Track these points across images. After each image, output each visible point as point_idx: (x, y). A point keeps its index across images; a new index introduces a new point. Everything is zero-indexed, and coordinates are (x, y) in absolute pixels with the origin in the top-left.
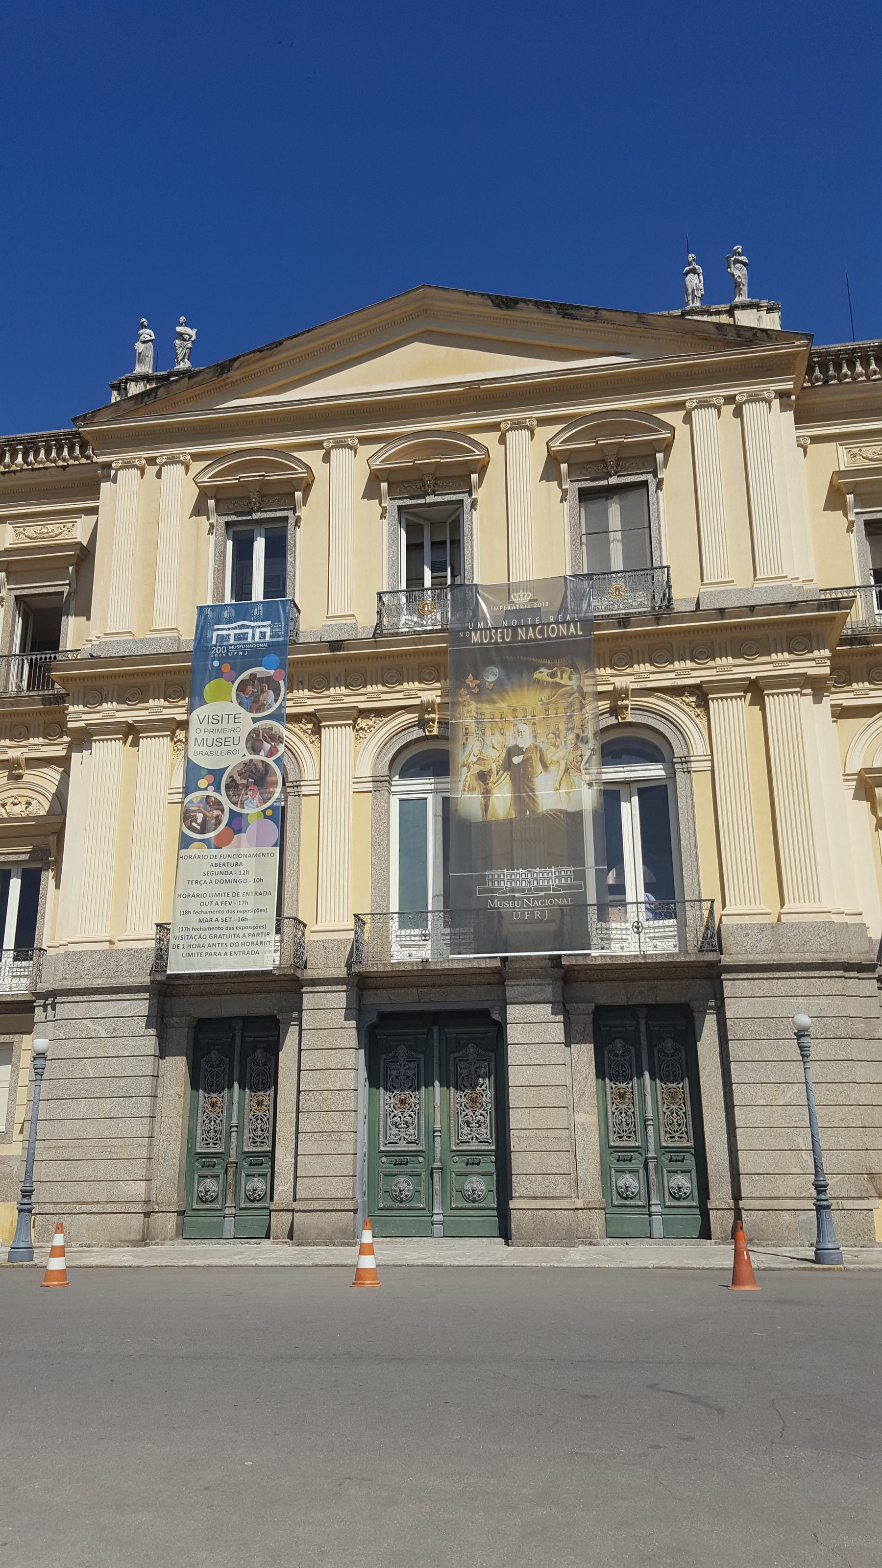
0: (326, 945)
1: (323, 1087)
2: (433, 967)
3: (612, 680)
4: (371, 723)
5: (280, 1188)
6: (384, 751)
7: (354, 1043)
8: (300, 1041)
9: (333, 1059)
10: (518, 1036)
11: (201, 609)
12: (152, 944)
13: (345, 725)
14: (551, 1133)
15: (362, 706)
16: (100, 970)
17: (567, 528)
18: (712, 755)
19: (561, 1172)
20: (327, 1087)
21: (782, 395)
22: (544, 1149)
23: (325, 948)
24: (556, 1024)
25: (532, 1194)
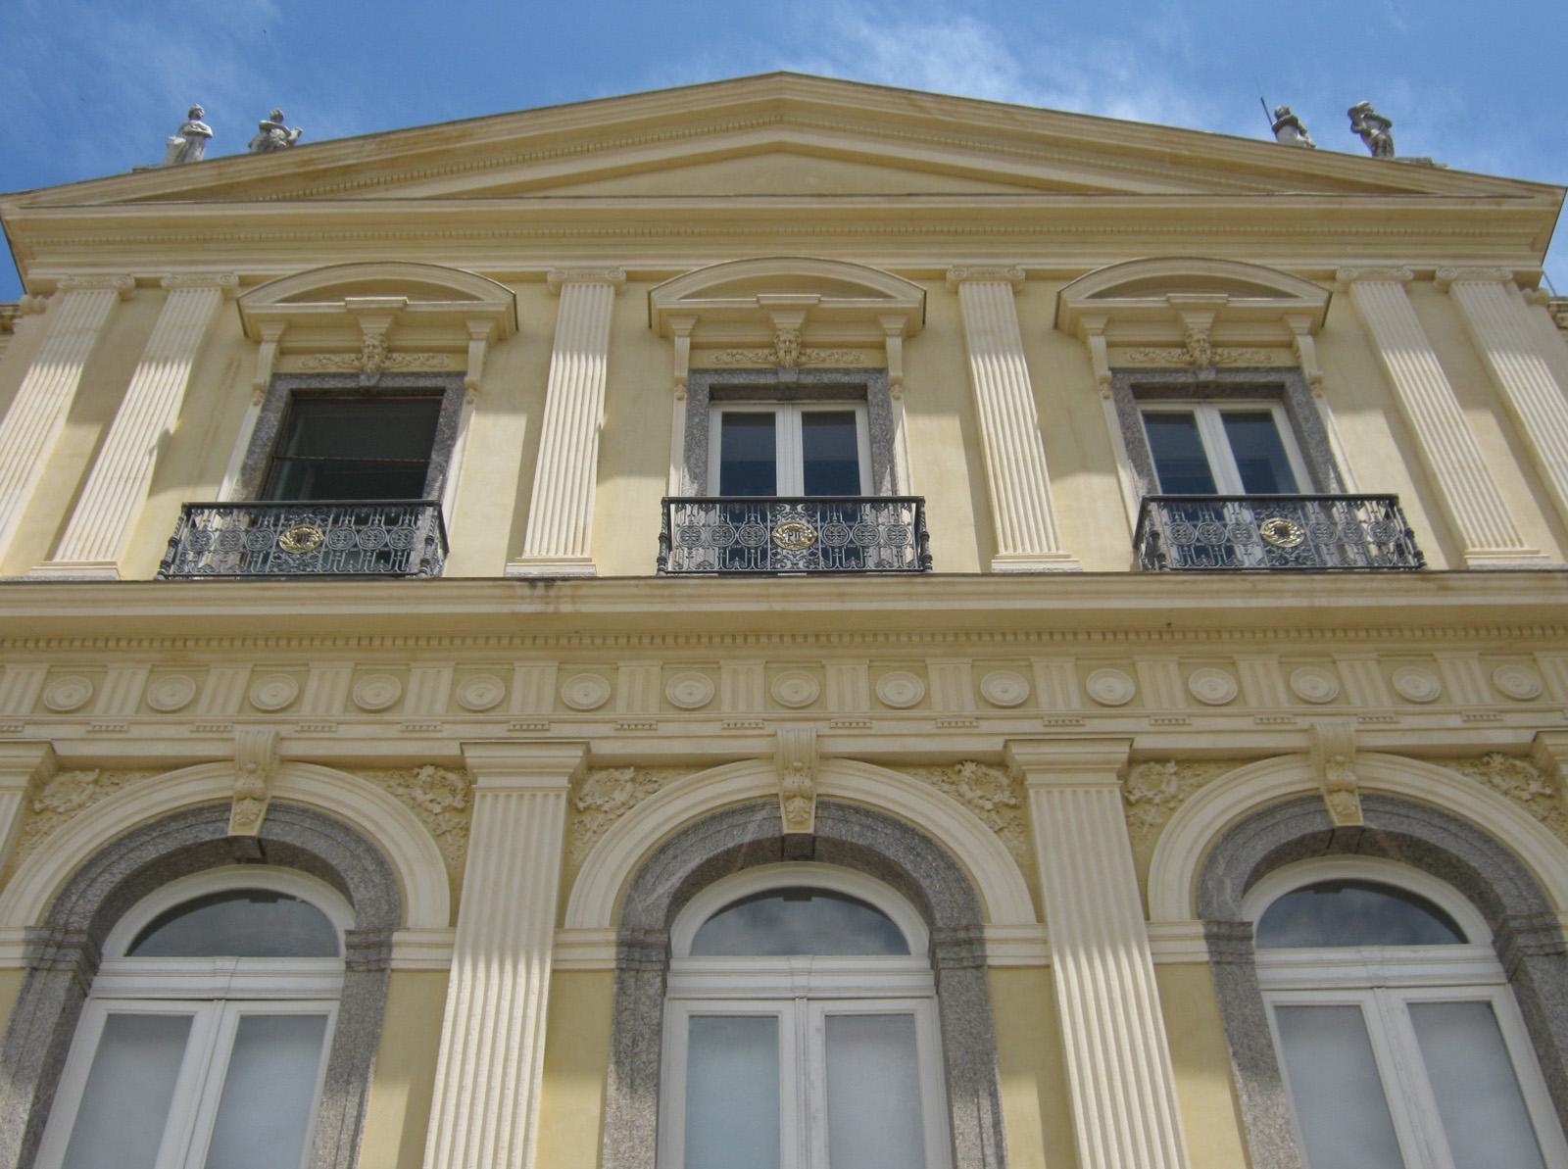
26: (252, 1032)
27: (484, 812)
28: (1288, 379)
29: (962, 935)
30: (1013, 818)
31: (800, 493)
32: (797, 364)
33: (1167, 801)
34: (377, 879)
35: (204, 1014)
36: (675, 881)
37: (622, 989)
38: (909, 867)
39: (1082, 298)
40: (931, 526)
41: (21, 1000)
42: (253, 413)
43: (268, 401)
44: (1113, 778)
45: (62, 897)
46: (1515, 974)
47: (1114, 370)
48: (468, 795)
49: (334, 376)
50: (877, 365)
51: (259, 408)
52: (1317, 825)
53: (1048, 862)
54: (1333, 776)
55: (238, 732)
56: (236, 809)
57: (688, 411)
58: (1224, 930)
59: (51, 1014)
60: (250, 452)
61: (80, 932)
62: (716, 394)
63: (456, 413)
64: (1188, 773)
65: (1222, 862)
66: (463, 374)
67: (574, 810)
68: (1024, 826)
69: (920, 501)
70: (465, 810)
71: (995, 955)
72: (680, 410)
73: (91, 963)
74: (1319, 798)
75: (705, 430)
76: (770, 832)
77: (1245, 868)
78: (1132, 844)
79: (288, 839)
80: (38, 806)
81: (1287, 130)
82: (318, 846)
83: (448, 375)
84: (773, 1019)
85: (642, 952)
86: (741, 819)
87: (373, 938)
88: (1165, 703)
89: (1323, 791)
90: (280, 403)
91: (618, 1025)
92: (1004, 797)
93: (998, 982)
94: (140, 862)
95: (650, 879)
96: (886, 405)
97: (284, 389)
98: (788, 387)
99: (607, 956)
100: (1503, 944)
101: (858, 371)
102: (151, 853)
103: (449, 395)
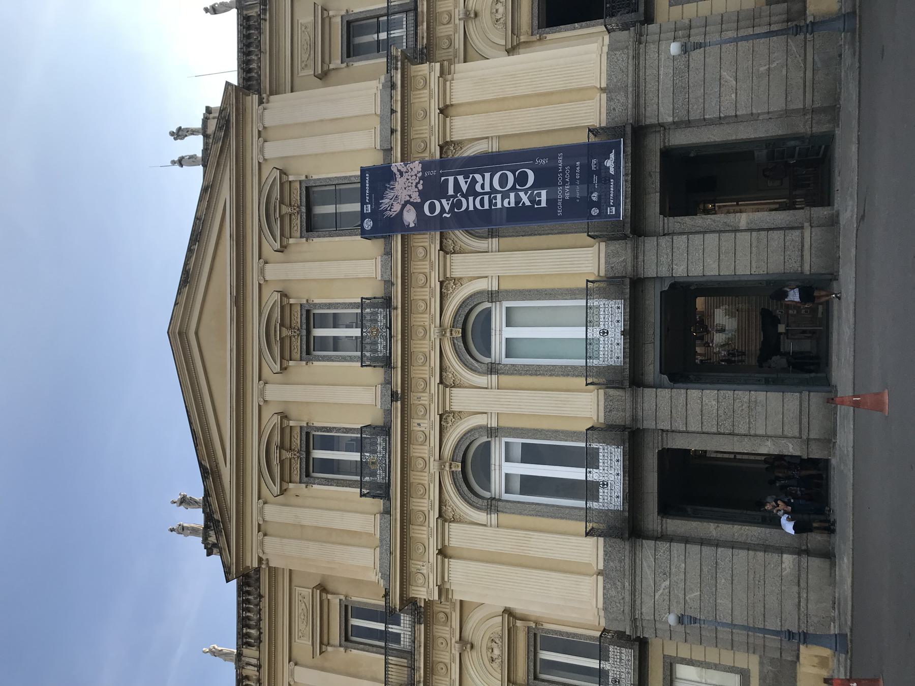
4: (450, 375)
11: (362, 495)
12: (601, 540)
13: (450, 393)
15: (438, 381)
16: (619, 583)
17: (330, 239)
21: (261, 102)
27: (455, 408)
28: (304, 185)
30: (458, 281)
35: (504, 472)
36: (474, 362)
44: (448, 256)
45: (478, 508)
48: (450, 412)
53: (471, 274)
55: (432, 471)
56: (453, 469)
59: (508, 505)
62: (308, 353)
68: (460, 278)
69: (362, 298)
70: (454, 412)
71: (495, 288)
81: (183, 162)
82: (463, 448)
85: (493, 369)
91: (512, 374)
93: (502, 287)
96: (315, 305)
97: (305, 479)
99: (494, 377)
102: (465, 489)
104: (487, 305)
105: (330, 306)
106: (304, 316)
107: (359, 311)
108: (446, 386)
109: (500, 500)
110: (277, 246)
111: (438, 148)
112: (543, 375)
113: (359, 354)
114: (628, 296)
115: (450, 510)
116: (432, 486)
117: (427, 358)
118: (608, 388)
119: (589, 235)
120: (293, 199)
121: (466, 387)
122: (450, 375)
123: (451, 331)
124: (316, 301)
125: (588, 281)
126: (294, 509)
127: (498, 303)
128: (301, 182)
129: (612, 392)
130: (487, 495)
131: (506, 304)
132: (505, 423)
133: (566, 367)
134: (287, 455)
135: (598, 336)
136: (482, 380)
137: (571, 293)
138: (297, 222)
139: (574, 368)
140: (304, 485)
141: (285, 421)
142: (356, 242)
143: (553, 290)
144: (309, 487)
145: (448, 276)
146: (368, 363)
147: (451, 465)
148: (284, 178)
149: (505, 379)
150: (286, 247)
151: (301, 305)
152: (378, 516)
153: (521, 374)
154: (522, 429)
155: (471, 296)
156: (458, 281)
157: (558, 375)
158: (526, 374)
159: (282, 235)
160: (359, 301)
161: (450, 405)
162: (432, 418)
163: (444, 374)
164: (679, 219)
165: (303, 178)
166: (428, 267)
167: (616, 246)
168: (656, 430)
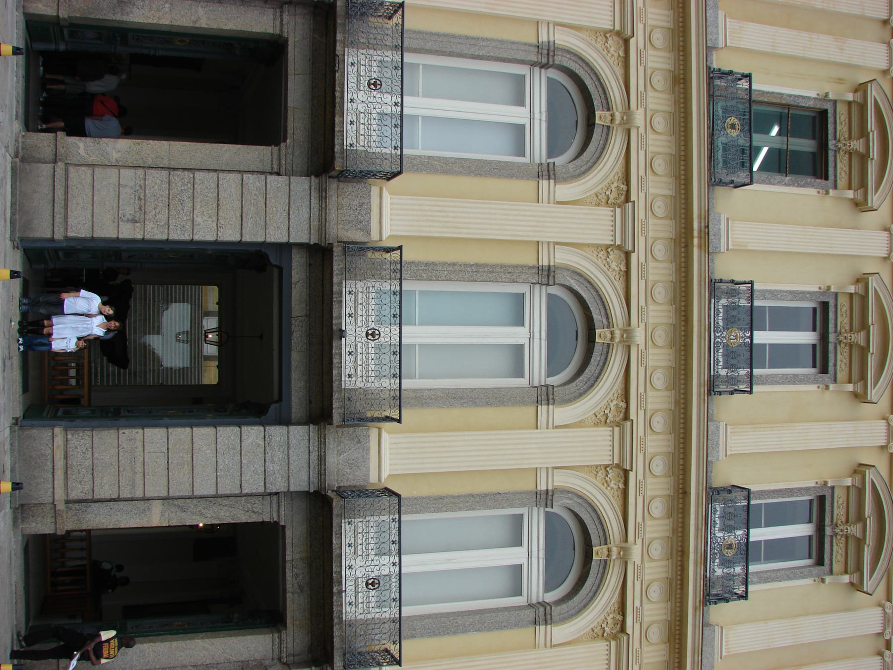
0: (365, 206)
1: (198, 200)
2: (335, 344)
3: (639, 541)
4: (613, 265)
5: (81, 145)
6: (581, 280)
7: (247, 238)
8: (252, 172)
9: (229, 214)
10: (251, 440)
11: (748, 77)
14: (139, 477)
18: (552, 646)
19: (96, 488)
20: (198, 206)
22: (121, 469)
23: (361, 205)
24: (262, 484)
25: (70, 453)
26: (519, 130)
27: (606, 212)
29: (551, 397)
31: (755, 342)
32: (840, 342)
33: (607, 482)
34: (578, 172)
36: (576, 287)
37: (530, 268)
38: (581, 378)
39: (872, 477)
40: (736, 396)
41: (525, 44)
42: (813, 94)
43: (820, 100)
46: (530, 606)
47: (833, 488)
48: (614, 205)
49: (835, 128)
50: (838, 380)
51: (815, 96)
52: (594, 539)
54: (615, 550)
56: (608, 114)
57: (813, 292)
58: (550, 497)
59: (520, 56)
60: (790, 96)
61: (554, 61)
63: (813, 186)
64: (619, 492)
65: (580, 501)
66: (835, 187)
67: (607, 247)
68: (597, 424)
69: (751, 392)
71: (542, 409)
72: (814, 288)
73: (544, 66)
74: (606, 544)
75: (802, 299)
76: (597, 324)
77: (576, 510)
78: (588, 466)
79: (595, 135)
80: (608, 35)
83: (835, 181)
84: (522, 324)
85: (546, 275)
86: (603, 312)
87: (552, 173)
88: (651, 486)
89: (609, 545)
90: (819, 105)
91: (517, 266)
92: (610, 418)
93: (532, 409)
94: (584, 79)
95: (577, 277)
96: (815, 381)
97: (828, 107)
98: (827, 338)
99: (544, 262)
100: (543, 604)
101: (835, 370)
102: (588, 83)
103: (823, 182)
104: (554, 381)
105: (795, 380)
106: (831, 364)
107: (756, 371)
108: (619, 247)
109: (533, 64)
110: (870, 475)
111: (629, 630)
112: (467, 265)
113: (757, 303)
114: (335, 396)
115: (612, 50)
116: (641, 88)
117: (649, 294)
118: (365, 243)
119: (398, 496)
120: (842, 545)
121: (588, 245)
122: (613, 265)
123: (612, 339)
124: (813, 387)
125: (399, 421)
126: (844, 59)
127: (536, 384)
128: (831, 572)
129: (358, 236)
130: (553, 74)
131: (522, 382)
132: (527, 186)
133: (429, 279)
134: (857, 145)
135: (382, 330)
136: (562, 257)
137: (425, 399)
138: (838, 510)
139: (417, 278)
140: (831, 97)
141: (860, 197)
142: (760, 481)
143: (451, 405)
144: (822, 94)
145: (617, 429)
146: (743, 287)
147: (612, 121)
148: (855, 578)
149: (527, 258)
150: (855, 472)
151: (835, 380)
152: (721, 44)
153: (502, 266)
154: (500, 176)
155: (581, 395)
156: (603, 421)
157: (443, 264)
158: (494, 266)
159: (861, 491)
160: (756, 388)
161: (614, 216)
162: (642, 195)
163: (623, 268)
164: (253, 520)
165: (828, 579)
166: (649, 444)
167: (350, 479)
168: (290, 174)
